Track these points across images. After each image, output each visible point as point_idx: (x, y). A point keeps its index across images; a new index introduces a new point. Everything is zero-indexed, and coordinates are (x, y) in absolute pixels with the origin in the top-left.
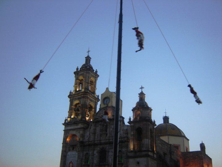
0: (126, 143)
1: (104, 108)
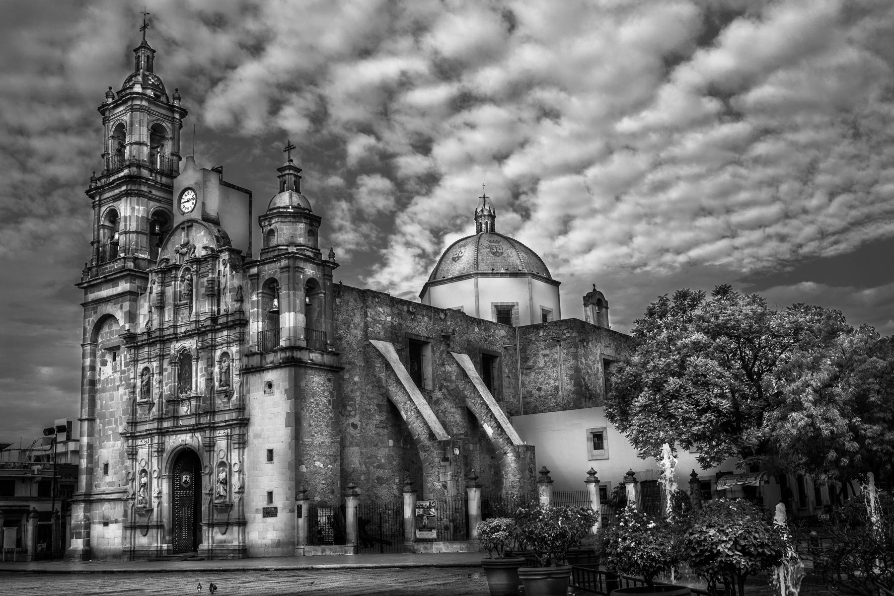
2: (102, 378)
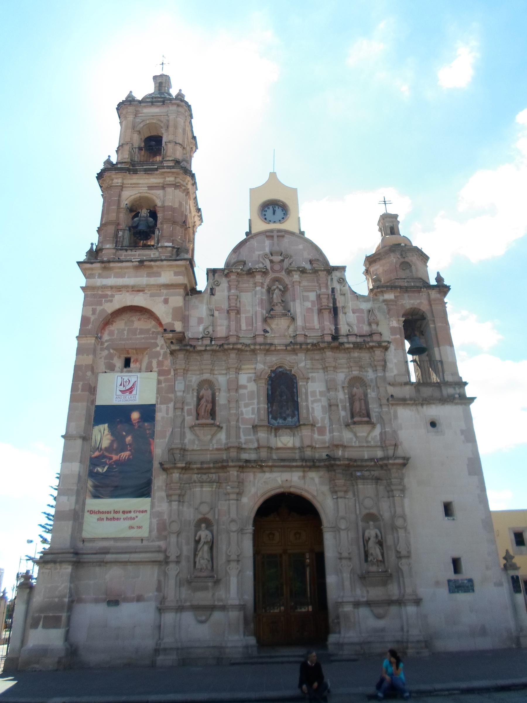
0: (378, 353)
1: (268, 234)
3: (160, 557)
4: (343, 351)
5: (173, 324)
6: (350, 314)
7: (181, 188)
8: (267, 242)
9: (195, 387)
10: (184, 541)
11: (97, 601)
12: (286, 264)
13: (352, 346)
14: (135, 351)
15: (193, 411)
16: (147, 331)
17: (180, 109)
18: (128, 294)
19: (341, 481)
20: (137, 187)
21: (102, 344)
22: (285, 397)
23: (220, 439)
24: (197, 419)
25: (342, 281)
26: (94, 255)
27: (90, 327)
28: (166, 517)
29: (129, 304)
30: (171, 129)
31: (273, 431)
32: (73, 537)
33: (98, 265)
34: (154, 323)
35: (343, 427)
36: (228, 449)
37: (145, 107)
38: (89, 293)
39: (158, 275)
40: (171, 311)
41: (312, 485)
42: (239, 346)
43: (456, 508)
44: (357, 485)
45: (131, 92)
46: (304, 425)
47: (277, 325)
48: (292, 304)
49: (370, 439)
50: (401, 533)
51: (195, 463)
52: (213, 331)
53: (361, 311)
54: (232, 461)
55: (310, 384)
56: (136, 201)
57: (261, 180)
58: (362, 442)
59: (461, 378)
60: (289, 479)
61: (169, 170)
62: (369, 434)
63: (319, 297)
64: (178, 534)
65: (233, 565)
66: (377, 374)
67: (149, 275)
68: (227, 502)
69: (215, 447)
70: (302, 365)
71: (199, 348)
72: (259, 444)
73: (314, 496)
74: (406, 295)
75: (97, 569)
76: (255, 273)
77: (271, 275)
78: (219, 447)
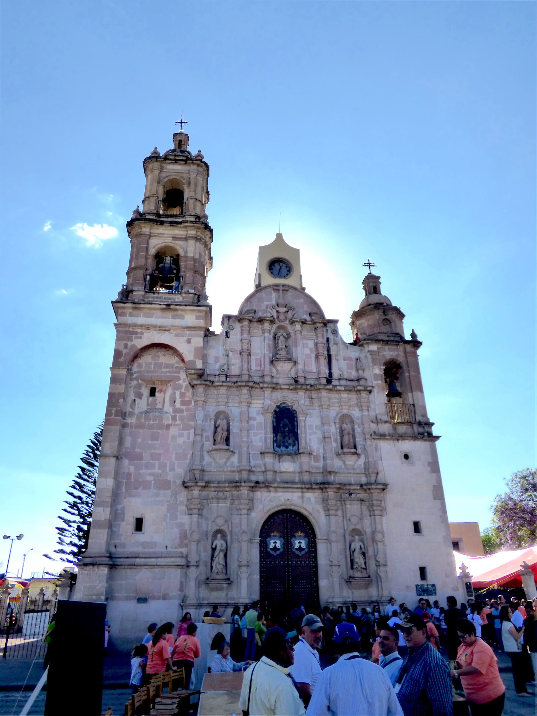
0: (364, 394)
1: (275, 288)
2: (136, 412)
3: (183, 562)
4: (335, 392)
5: (195, 362)
6: (342, 361)
7: (201, 241)
8: (274, 295)
9: (213, 416)
10: (202, 548)
11: (127, 598)
12: (290, 314)
13: (343, 388)
14: (160, 383)
15: (210, 438)
16: (171, 366)
17: (200, 169)
18: (155, 332)
19: (333, 501)
20: (162, 237)
21: (132, 374)
22: (287, 429)
23: (233, 462)
24: (214, 444)
25: (335, 332)
26: (126, 294)
27: (122, 359)
28: (187, 527)
29: (156, 341)
30: (192, 186)
31: (277, 457)
32: (108, 544)
33: (130, 305)
34: (177, 359)
35: (335, 455)
36: (240, 471)
37: (169, 163)
38: (121, 329)
39: (182, 317)
40: (193, 350)
41: (309, 503)
42: (251, 384)
43: (423, 526)
44: (345, 505)
45: (156, 148)
46: (303, 453)
47: (282, 367)
48: (294, 349)
49: (356, 467)
50: (380, 546)
51: (213, 482)
52: (228, 369)
53: (350, 359)
54: (245, 482)
55: (308, 418)
56: (161, 249)
57: (269, 239)
58: (349, 469)
59: (428, 419)
60: (290, 498)
61: (191, 225)
62: (355, 463)
63: (316, 344)
64: (198, 542)
65: (244, 569)
66: (362, 412)
67: (174, 317)
68: (239, 516)
69: (229, 469)
70: (302, 402)
71: (216, 384)
72: (266, 468)
73: (310, 513)
74: (387, 347)
75: (129, 571)
76: (264, 321)
77: (278, 324)
78: (233, 469)
